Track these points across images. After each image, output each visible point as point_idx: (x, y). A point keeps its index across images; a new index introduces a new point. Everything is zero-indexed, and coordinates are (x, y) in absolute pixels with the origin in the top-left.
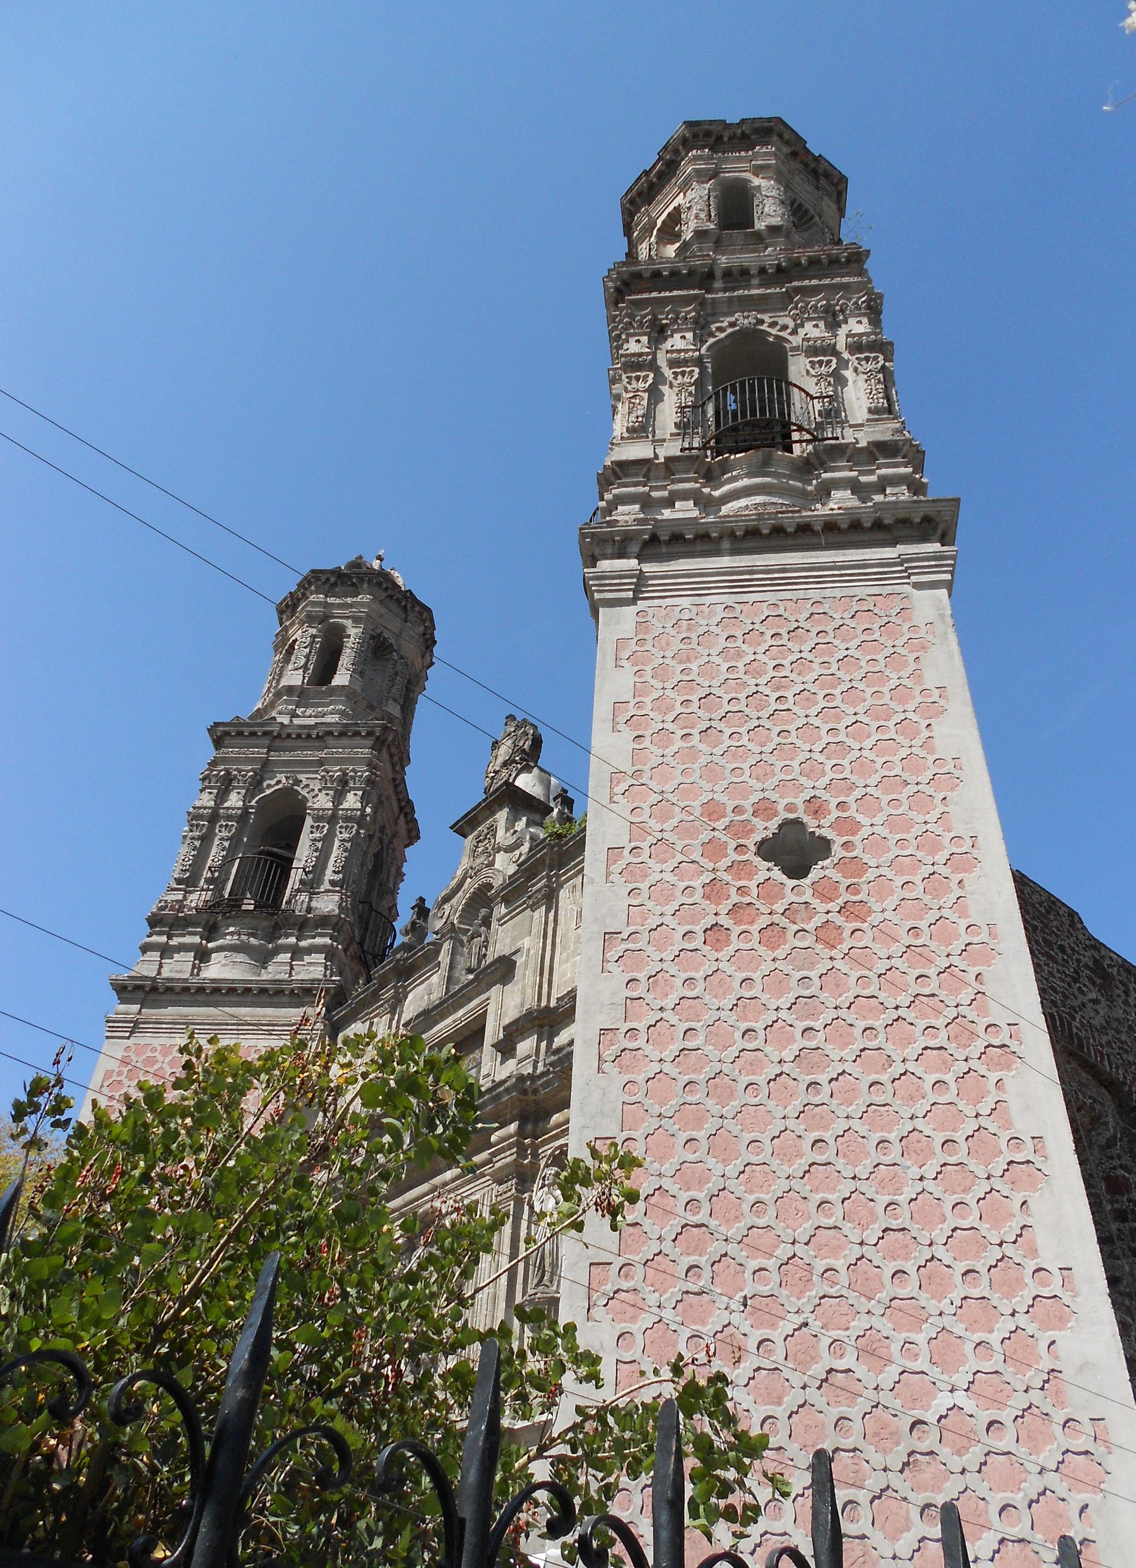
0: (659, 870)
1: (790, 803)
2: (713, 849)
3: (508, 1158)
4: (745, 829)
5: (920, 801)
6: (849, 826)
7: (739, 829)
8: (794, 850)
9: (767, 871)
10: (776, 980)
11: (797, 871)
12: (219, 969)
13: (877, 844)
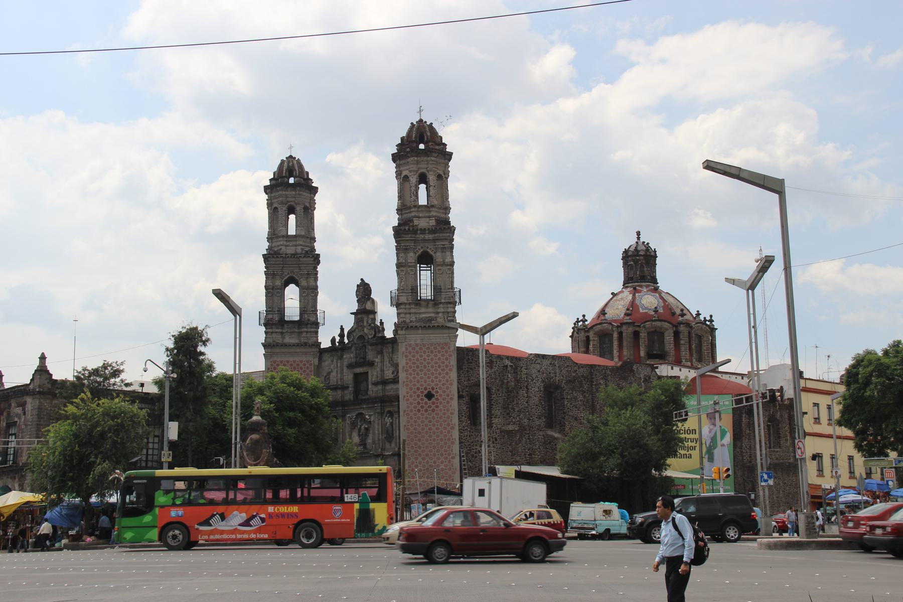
0: (411, 400)
1: (429, 388)
2: (418, 396)
3: (379, 411)
4: (422, 392)
5: (448, 388)
6: (437, 392)
7: (422, 392)
8: (429, 396)
9: (426, 400)
10: (426, 418)
11: (429, 399)
12: (287, 340)
13: (441, 396)
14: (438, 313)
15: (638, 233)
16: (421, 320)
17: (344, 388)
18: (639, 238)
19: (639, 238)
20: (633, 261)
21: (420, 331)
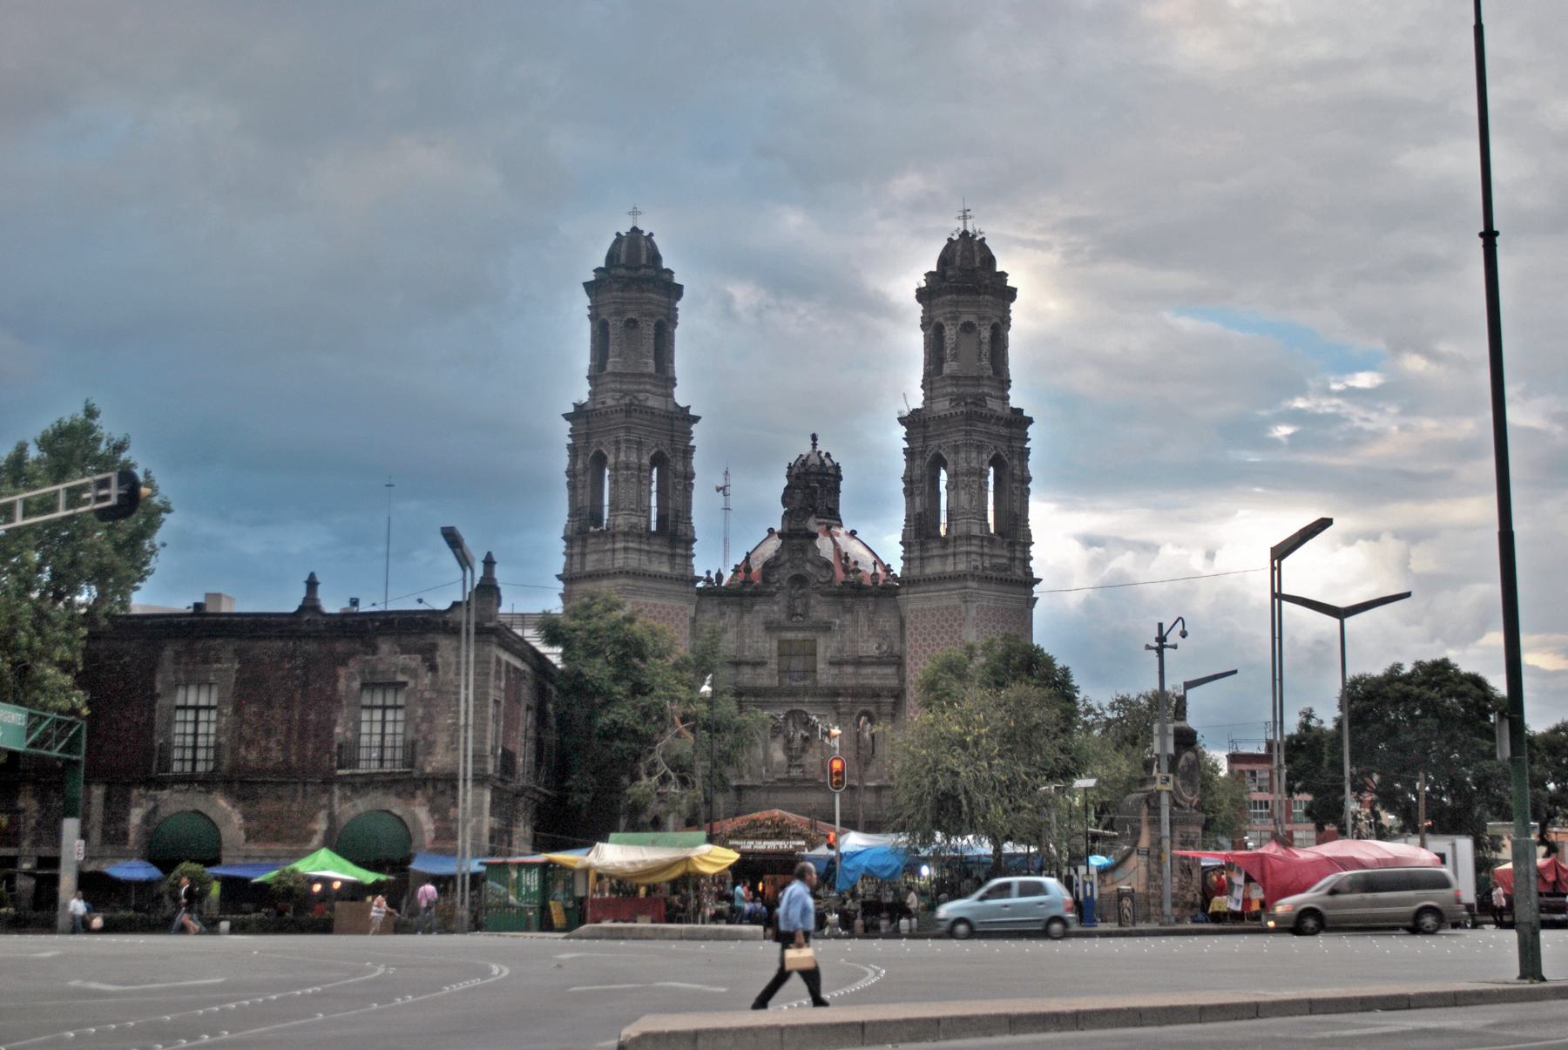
14: (1012, 559)
15: (814, 438)
16: (994, 567)
17: (757, 664)
18: (814, 445)
19: (814, 445)
20: (819, 482)
21: (993, 586)
